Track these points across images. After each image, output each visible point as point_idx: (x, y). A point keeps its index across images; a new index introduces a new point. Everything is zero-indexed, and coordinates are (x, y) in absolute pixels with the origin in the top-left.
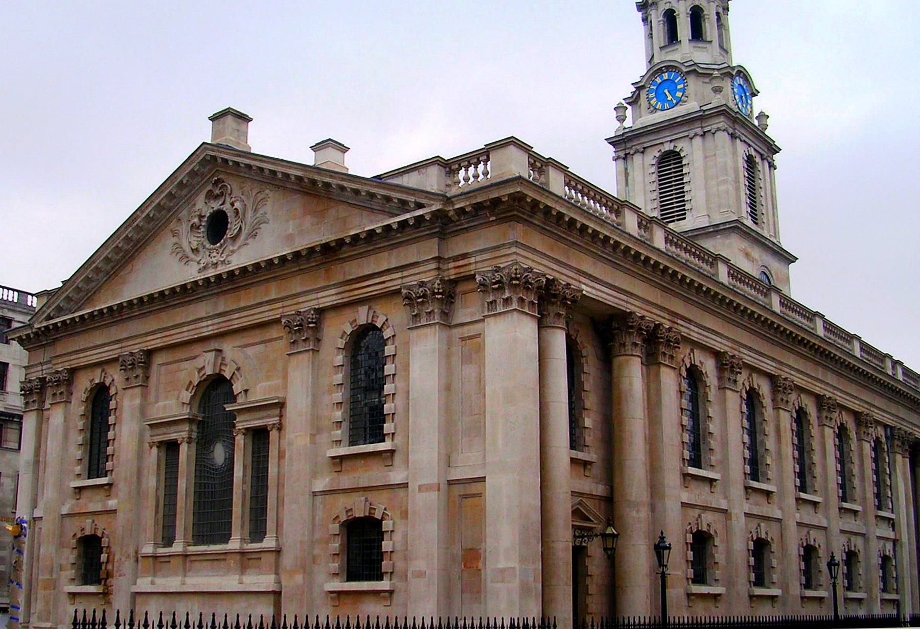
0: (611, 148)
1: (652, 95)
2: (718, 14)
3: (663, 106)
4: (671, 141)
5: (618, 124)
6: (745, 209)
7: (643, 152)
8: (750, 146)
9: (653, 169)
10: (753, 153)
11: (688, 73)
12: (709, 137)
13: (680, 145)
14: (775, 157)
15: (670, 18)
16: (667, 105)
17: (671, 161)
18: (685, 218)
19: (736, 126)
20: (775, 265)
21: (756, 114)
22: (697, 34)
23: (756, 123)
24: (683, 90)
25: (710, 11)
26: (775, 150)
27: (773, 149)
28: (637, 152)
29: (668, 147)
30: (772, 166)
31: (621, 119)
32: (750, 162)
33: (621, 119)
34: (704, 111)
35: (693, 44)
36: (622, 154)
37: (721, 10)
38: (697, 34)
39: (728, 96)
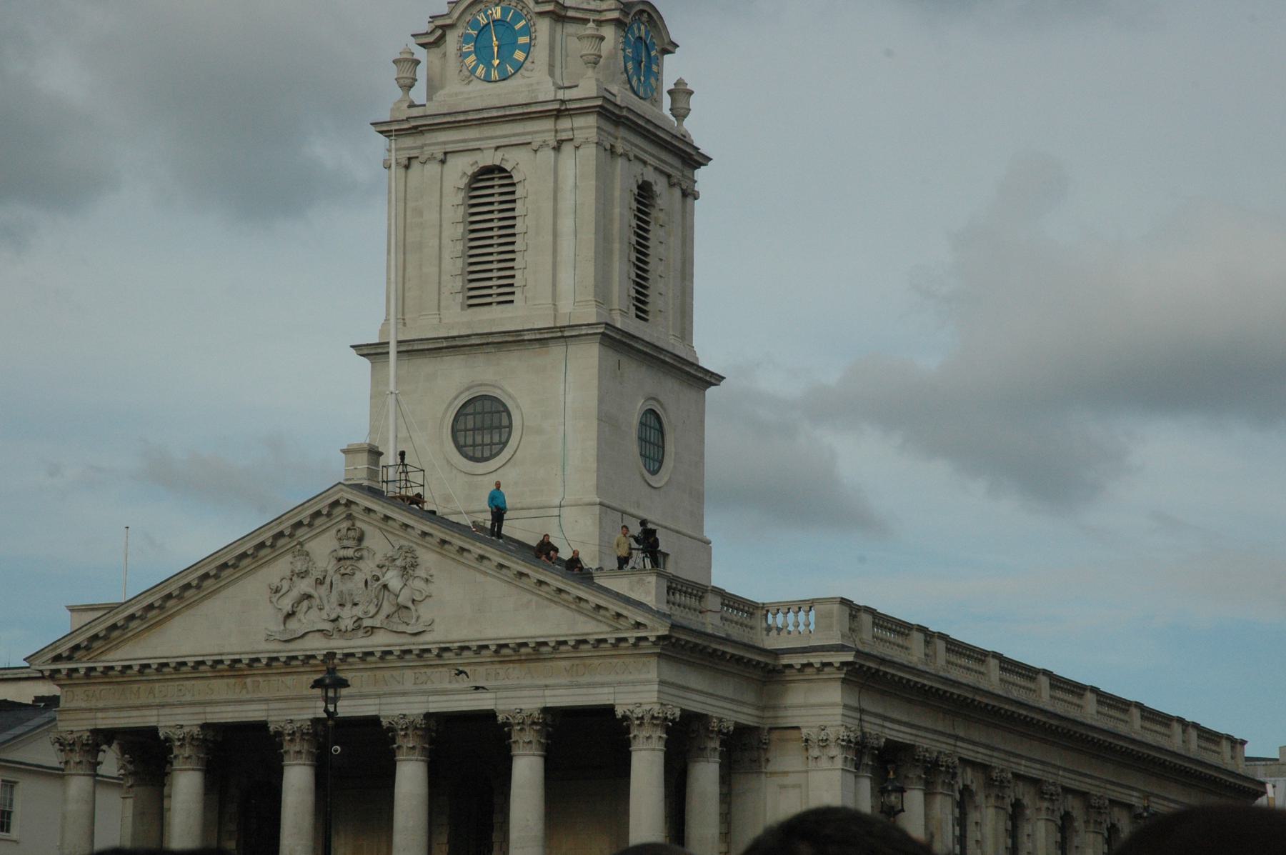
1: (469, 47)
3: (488, 73)
4: (497, 148)
5: (399, 93)
7: (443, 162)
8: (645, 163)
9: (461, 195)
10: (650, 175)
11: (541, 14)
12: (567, 149)
13: (516, 161)
14: (700, 174)
16: (495, 75)
18: (512, 302)
20: (671, 394)
21: (668, 84)
24: (527, 49)
26: (703, 160)
27: (692, 159)
28: (432, 158)
30: (689, 194)
32: (644, 193)
34: (563, 102)
36: (403, 156)
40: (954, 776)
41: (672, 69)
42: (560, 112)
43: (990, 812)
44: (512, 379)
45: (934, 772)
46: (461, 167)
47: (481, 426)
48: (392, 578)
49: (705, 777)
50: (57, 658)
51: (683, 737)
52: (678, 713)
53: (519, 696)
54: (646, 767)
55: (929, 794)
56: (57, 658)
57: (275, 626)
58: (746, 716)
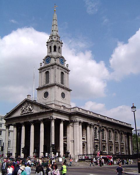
0: (39, 71)
2: (59, 47)
6: (59, 82)
10: (63, 72)
15: (50, 47)
17: (47, 73)
19: (59, 67)
22: (55, 50)
23: (66, 66)
25: (57, 46)
26: (69, 71)
29: (47, 70)
31: (41, 66)
32: (62, 73)
33: (41, 66)
35: (54, 52)
37: (60, 46)
38: (55, 50)
39: (58, 62)
40: (94, 126)
41: (66, 63)
42: (52, 65)
43: (106, 132)
44: (49, 90)
45: (91, 126)
46: (44, 72)
47: (46, 95)
48: (30, 107)
49: (62, 125)
50: (5, 118)
51: (58, 122)
52: (56, 118)
53: (40, 118)
54: (53, 124)
55: (90, 128)
56: (5, 118)
57: (21, 113)
58: (67, 119)
